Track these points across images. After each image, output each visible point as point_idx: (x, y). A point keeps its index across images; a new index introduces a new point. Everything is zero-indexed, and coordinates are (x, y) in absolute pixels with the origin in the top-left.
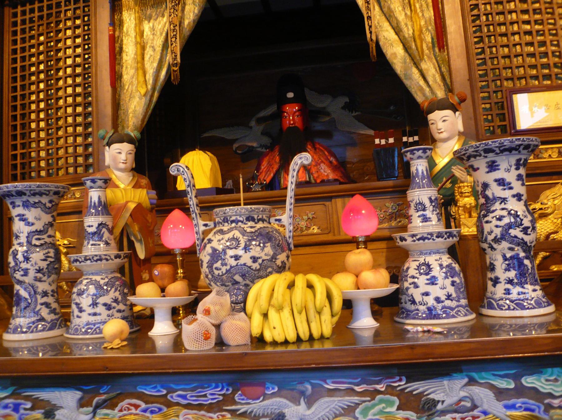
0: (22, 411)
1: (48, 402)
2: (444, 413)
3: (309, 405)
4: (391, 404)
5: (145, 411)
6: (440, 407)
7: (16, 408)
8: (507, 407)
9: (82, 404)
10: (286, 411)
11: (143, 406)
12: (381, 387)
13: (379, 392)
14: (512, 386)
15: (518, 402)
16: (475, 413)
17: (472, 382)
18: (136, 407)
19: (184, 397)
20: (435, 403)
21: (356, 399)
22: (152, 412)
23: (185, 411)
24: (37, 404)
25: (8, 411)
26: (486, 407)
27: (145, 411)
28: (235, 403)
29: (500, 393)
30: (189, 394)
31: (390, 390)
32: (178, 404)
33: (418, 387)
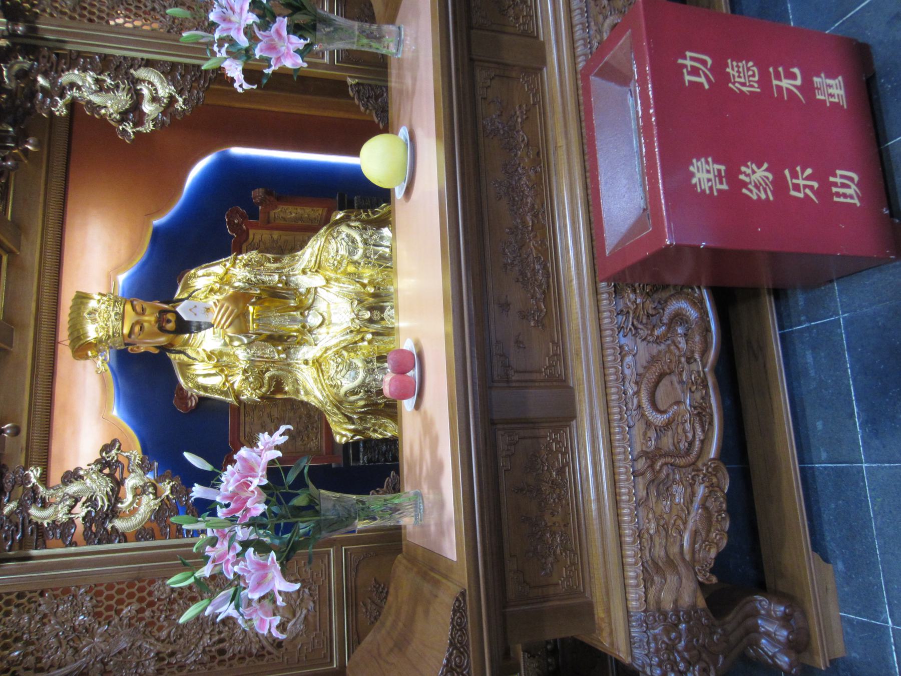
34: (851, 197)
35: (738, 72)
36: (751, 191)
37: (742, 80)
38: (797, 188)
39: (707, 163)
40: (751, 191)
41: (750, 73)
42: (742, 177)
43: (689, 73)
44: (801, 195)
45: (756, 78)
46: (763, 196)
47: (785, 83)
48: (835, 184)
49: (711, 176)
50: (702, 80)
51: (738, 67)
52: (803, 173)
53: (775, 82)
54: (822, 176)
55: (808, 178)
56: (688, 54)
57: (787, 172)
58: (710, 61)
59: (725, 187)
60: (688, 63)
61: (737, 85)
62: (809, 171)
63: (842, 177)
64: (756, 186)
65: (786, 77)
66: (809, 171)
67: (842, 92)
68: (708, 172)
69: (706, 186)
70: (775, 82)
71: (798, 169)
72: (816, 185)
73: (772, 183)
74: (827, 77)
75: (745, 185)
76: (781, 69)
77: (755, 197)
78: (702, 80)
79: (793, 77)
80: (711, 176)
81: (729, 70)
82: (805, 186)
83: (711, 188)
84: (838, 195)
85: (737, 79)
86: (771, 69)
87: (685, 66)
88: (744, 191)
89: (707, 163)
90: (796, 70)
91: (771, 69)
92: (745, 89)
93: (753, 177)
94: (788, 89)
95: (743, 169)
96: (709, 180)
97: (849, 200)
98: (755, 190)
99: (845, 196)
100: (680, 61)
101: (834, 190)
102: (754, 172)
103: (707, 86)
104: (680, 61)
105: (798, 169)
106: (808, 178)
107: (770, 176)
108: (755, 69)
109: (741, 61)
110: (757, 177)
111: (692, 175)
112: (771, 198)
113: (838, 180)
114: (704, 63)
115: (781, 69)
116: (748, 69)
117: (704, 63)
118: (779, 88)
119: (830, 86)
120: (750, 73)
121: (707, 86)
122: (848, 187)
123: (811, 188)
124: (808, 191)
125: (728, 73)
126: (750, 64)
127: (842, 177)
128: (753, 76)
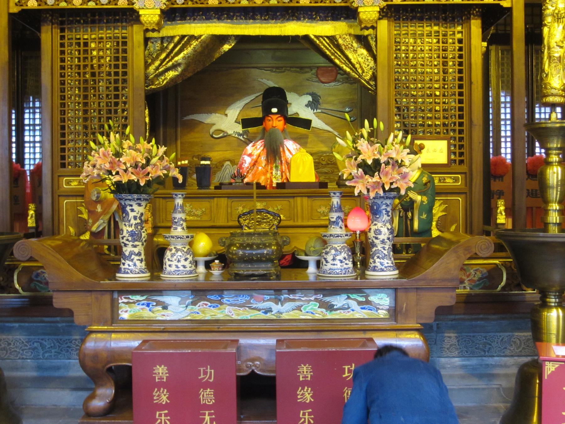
0: (151, 306)
1: (164, 302)
2: (337, 309)
3: (282, 305)
4: (316, 305)
5: (210, 306)
6: (335, 307)
7: (148, 305)
8: (362, 308)
9: (180, 303)
10: (272, 307)
11: (209, 304)
12: (312, 298)
13: (311, 301)
14: (364, 300)
15: (366, 306)
16: (349, 310)
17: (349, 298)
18: (206, 305)
19: (229, 301)
20: (333, 305)
21: (302, 303)
22: (214, 307)
23: (228, 307)
24: (158, 303)
25: (144, 306)
26: (353, 308)
27: (210, 306)
28: (251, 304)
29: (360, 303)
30: (231, 300)
31: (316, 300)
32: (226, 304)
33: (328, 299)
35: (209, 394)
36: (156, 392)
37: (205, 396)
39: (166, 373)
40: (156, 392)
41: (209, 400)
45: (207, 403)
49: (161, 374)
50: (202, 376)
51: (211, 394)
53: (207, 412)
56: (213, 371)
57: (166, 412)
58: (211, 380)
59: (157, 380)
61: (202, 393)
64: (159, 396)
65: (210, 418)
70: (207, 412)
73: (161, 403)
76: (214, 416)
77: (154, 394)
78: (202, 376)
81: (209, 390)
85: (205, 393)
86: (213, 411)
87: (207, 369)
88: (156, 389)
89: (166, 373)
91: (213, 411)
92: (201, 396)
94: (205, 418)
96: (159, 373)
98: (157, 394)
100: (209, 367)
102: (165, 395)
103: (200, 378)
104: (209, 367)
107: (164, 403)
108: (211, 403)
109: (214, 396)
111: (160, 366)
112: (155, 402)
114: (210, 378)
115: (214, 416)
116: (211, 400)
117: (210, 378)
118: (204, 414)
120: (209, 400)
121: (200, 378)
125: (207, 389)
126: (214, 401)
128: (208, 402)
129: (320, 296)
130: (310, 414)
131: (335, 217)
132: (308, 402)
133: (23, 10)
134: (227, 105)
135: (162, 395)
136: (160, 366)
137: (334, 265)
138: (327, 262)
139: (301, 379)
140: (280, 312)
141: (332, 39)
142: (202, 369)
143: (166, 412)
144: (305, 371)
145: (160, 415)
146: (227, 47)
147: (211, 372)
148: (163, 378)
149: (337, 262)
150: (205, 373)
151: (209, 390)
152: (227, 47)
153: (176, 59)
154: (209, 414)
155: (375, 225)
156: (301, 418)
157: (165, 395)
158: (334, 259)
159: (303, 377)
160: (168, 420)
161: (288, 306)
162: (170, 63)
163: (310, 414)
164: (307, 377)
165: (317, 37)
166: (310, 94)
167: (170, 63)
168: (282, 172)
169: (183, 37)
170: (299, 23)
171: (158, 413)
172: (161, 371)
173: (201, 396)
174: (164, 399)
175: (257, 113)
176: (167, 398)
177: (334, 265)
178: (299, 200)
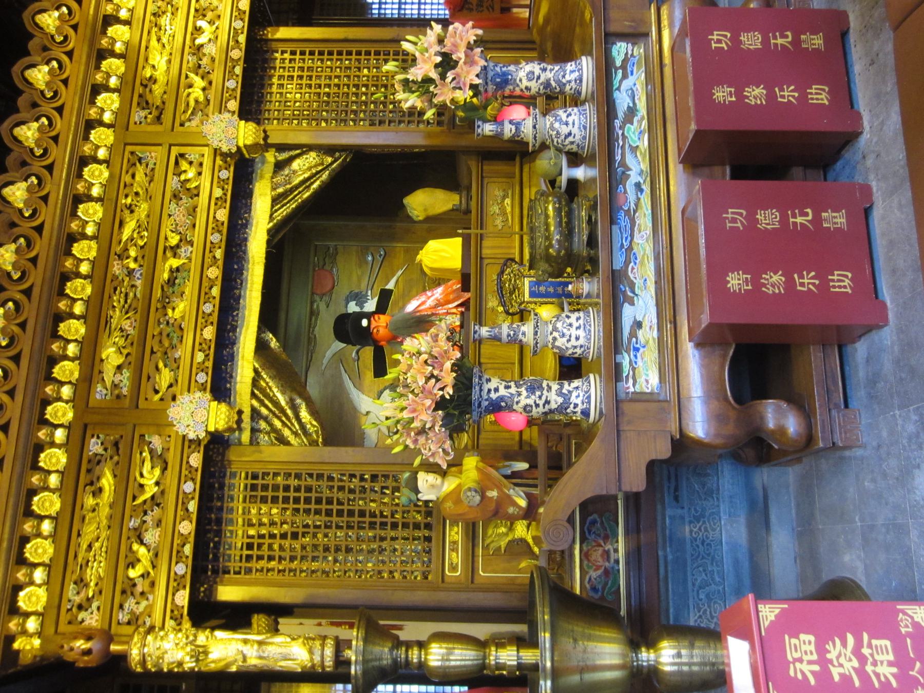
0: (638, 346)
1: (632, 327)
2: (634, 103)
3: (630, 169)
4: (629, 128)
5: (635, 263)
6: (631, 105)
7: (637, 350)
8: (632, 74)
9: (632, 304)
10: (633, 182)
11: (632, 264)
12: (620, 132)
13: (623, 134)
14: (620, 71)
15: (629, 69)
16: (635, 89)
17: (618, 89)
18: (633, 269)
19: (626, 238)
20: (629, 107)
21: (627, 146)
22: (636, 258)
23: (635, 239)
24: (633, 334)
25: (638, 355)
26: (632, 84)
27: (635, 263)
28: (629, 209)
29: (625, 76)
30: (625, 236)
32: (631, 242)
33: (621, 114)
34: (845, 287)
38: (802, 285)
40: (768, 289)
42: (763, 281)
43: (730, 222)
44: (805, 289)
46: (777, 291)
47: (799, 220)
48: (833, 281)
49: (741, 282)
50: (739, 225)
52: (808, 275)
53: (791, 220)
54: (823, 276)
55: (812, 278)
56: (730, 210)
57: (796, 276)
59: (750, 287)
60: (730, 216)
62: (813, 274)
63: (839, 275)
64: (773, 286)
65: (800, 216)
66: (813, 274)
67: (844, 220)
68: (739, 279)
69: (737, 288)
71: (805, 273)
72: (817, 282)
74: (833, 212)
75: (764, 285)
76: (797, 211)
77: (771, 292)
78: (739, 225)
79: (807, 214)
80: (741, 282)
81: (758, 216)
82: (808, 284)
83: (740, 289)
84: (834, 287)
87: (727, 218)
88: (764, 289)
89: (739, 274)
90: (809, 210)
92: (769, 227)
93: (771, 280)
95: (764, 276)
96: (739, 284)
97: (843, 290)
98: (771, 288)
99: (840, 287)
101: (831, 284)
102: (771, 277)
105: (805, 273)
106: (812, 278)
107: (783, 279)
110: (774, 280)
111: (729, 282)
113: (835, 278)
114: (741, 214)
115: (797, 211)
116: (772, 214)
117: (741, 214)
118: (795, 224)
119: (836, 217)
122: (843, 281)
123: (813, 284)
124: (811, 286)
127: (839, 275)
129: (617, 123)
130: (782, 90)
131: (510, 126)
132: (765, 92)
133: (189, 614)
134: (355, 410)
135: (771, 280)
136: (729, 282)
137: (574, 124)
138: (570, 134)
139: (734, 99)
140: (641, 173)
141: (275, 200)
142: (728, 225)
143: (796, 276)
144: (721, 94)
145: (802, 285)
146: (274, 344)
147: (733, 213)
148: (747, 278)
149: (570, 120)
150: (734, 220)
151: (758, 216)
152: (274, 344)
153: (283, 403)
154: (794, 216)
155: (521, 80)
156: (789, 101)
157: (771, 277)
158: (567, 124)
159: (731, 97)
160: (808, 275)
161: (630, 160)
162: (289, 412)
163: (782, 90)
164: (731, 92)
165: (271, 217)
166: (347, 303)
167: (289, 412)
168: (448, 313)
169: (253, 395)
170: (250, 239)
171: (799, 288)
172: (736, 281)
173: (769, 227)
174: (777, 278)
175: (368, 353)
176: (775, 273)
177: (574, 124)
178: (486, 252)
